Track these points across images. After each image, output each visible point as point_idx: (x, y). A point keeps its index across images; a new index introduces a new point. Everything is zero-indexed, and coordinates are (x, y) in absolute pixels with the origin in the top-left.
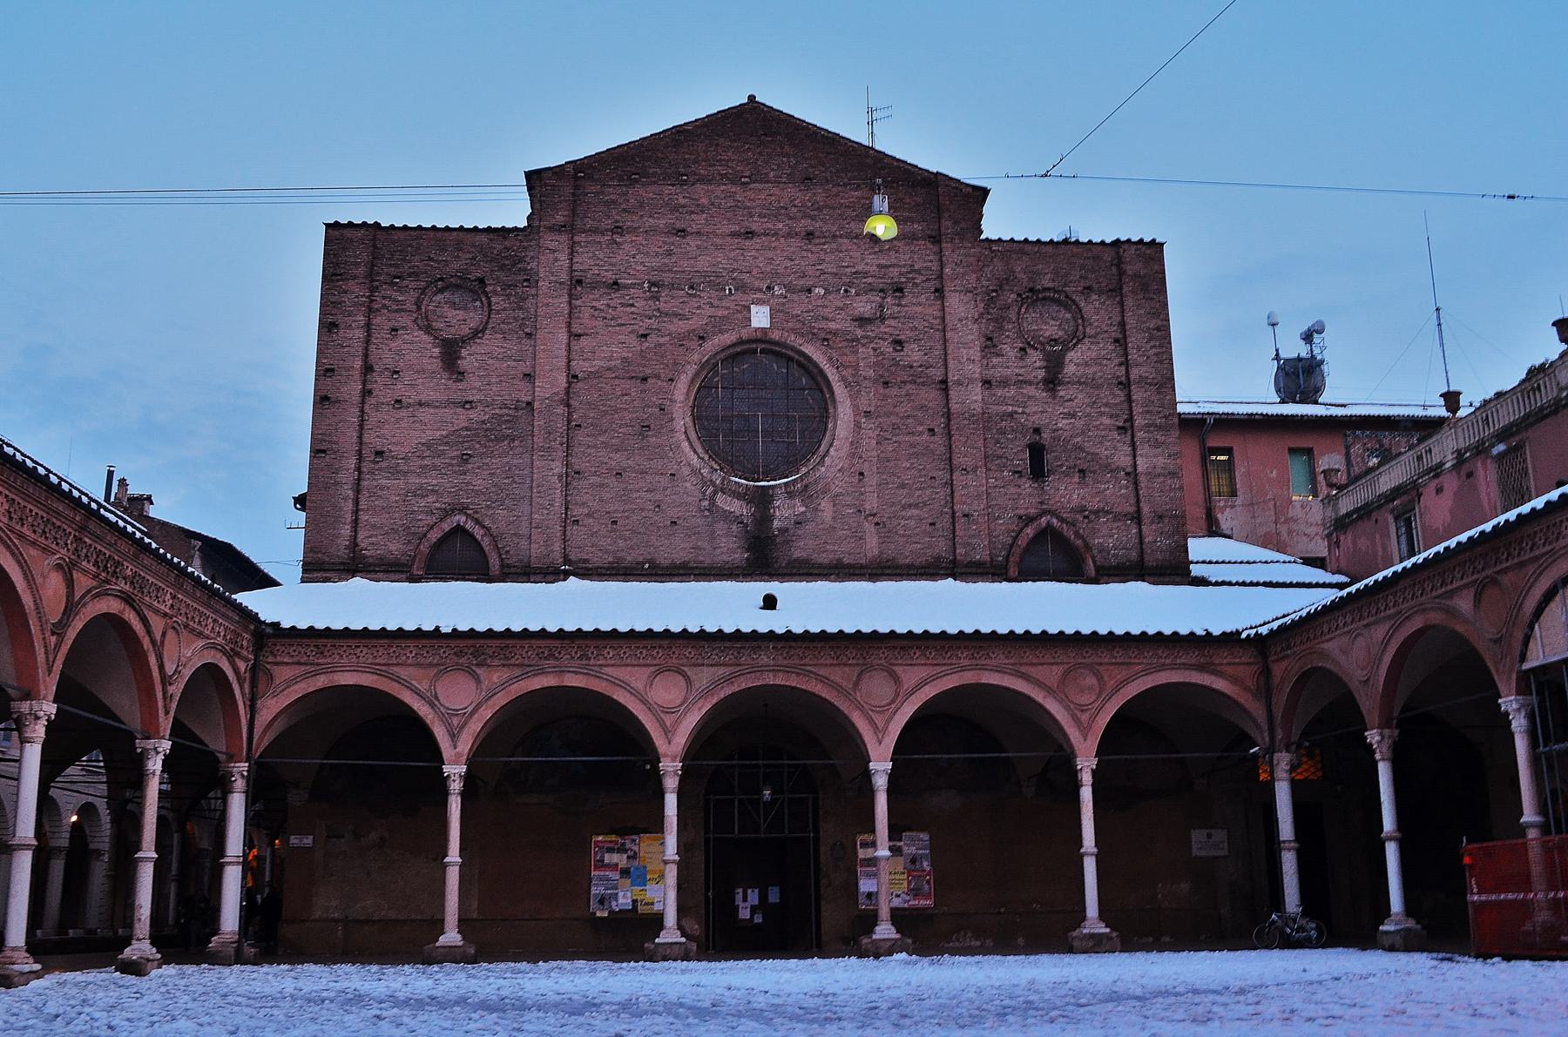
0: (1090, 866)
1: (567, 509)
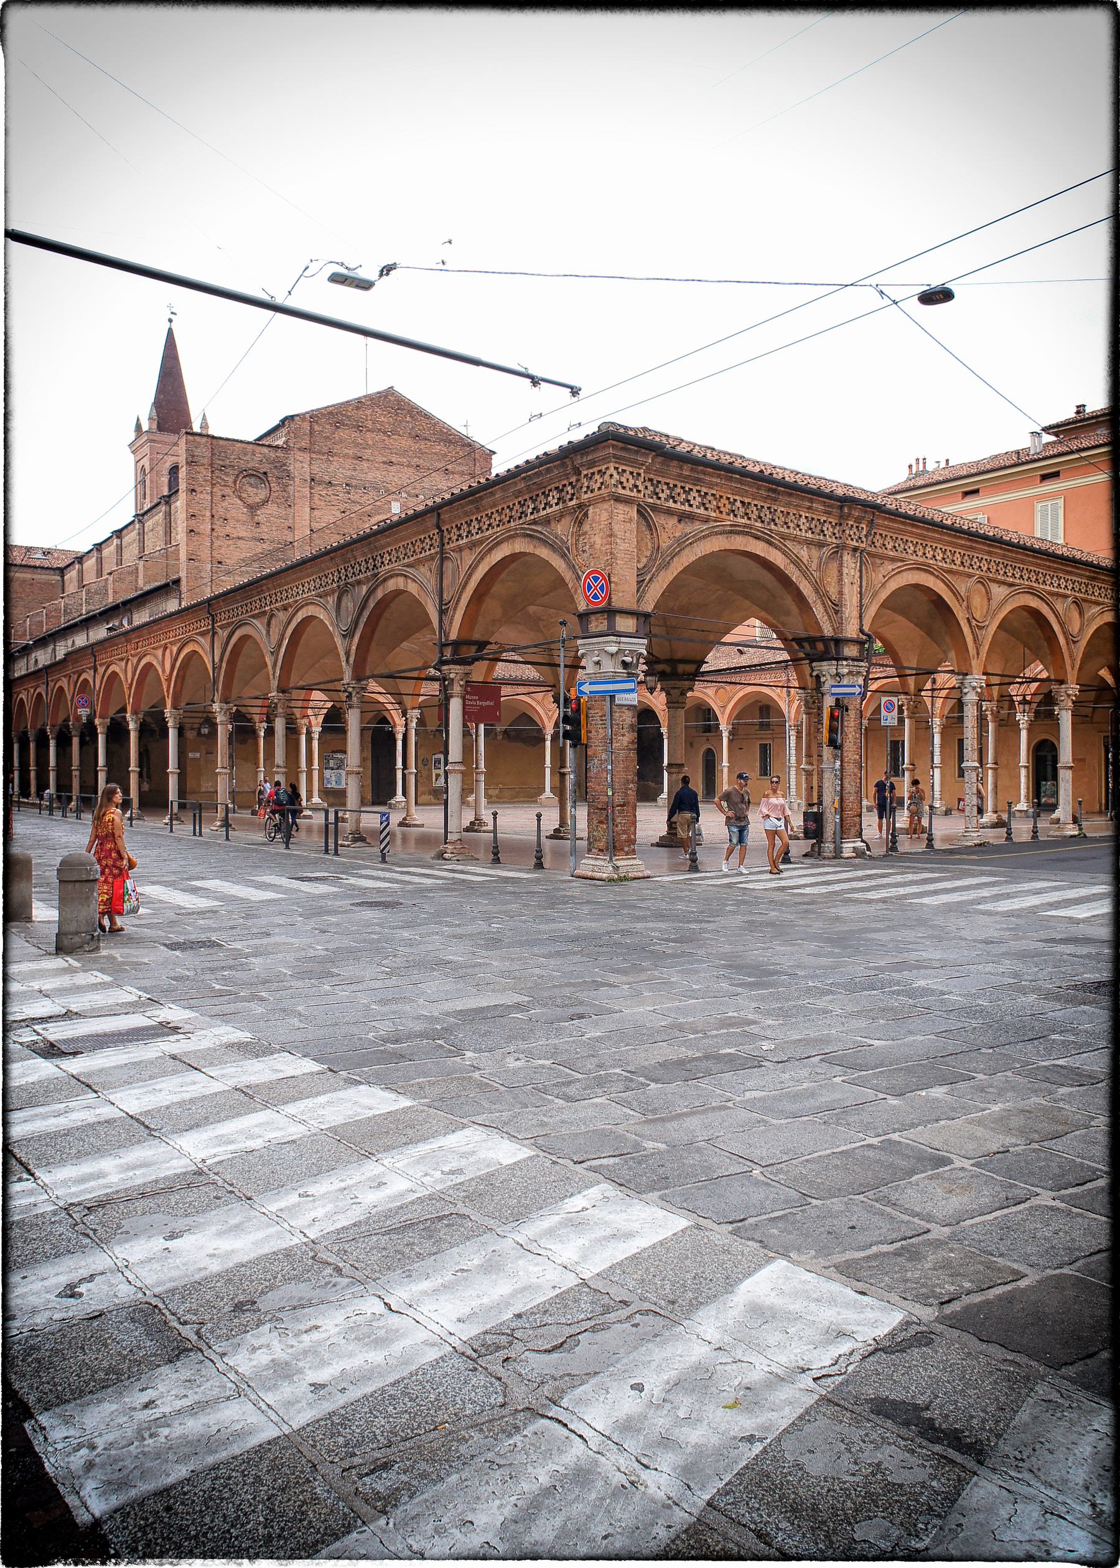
0: (548, 772)
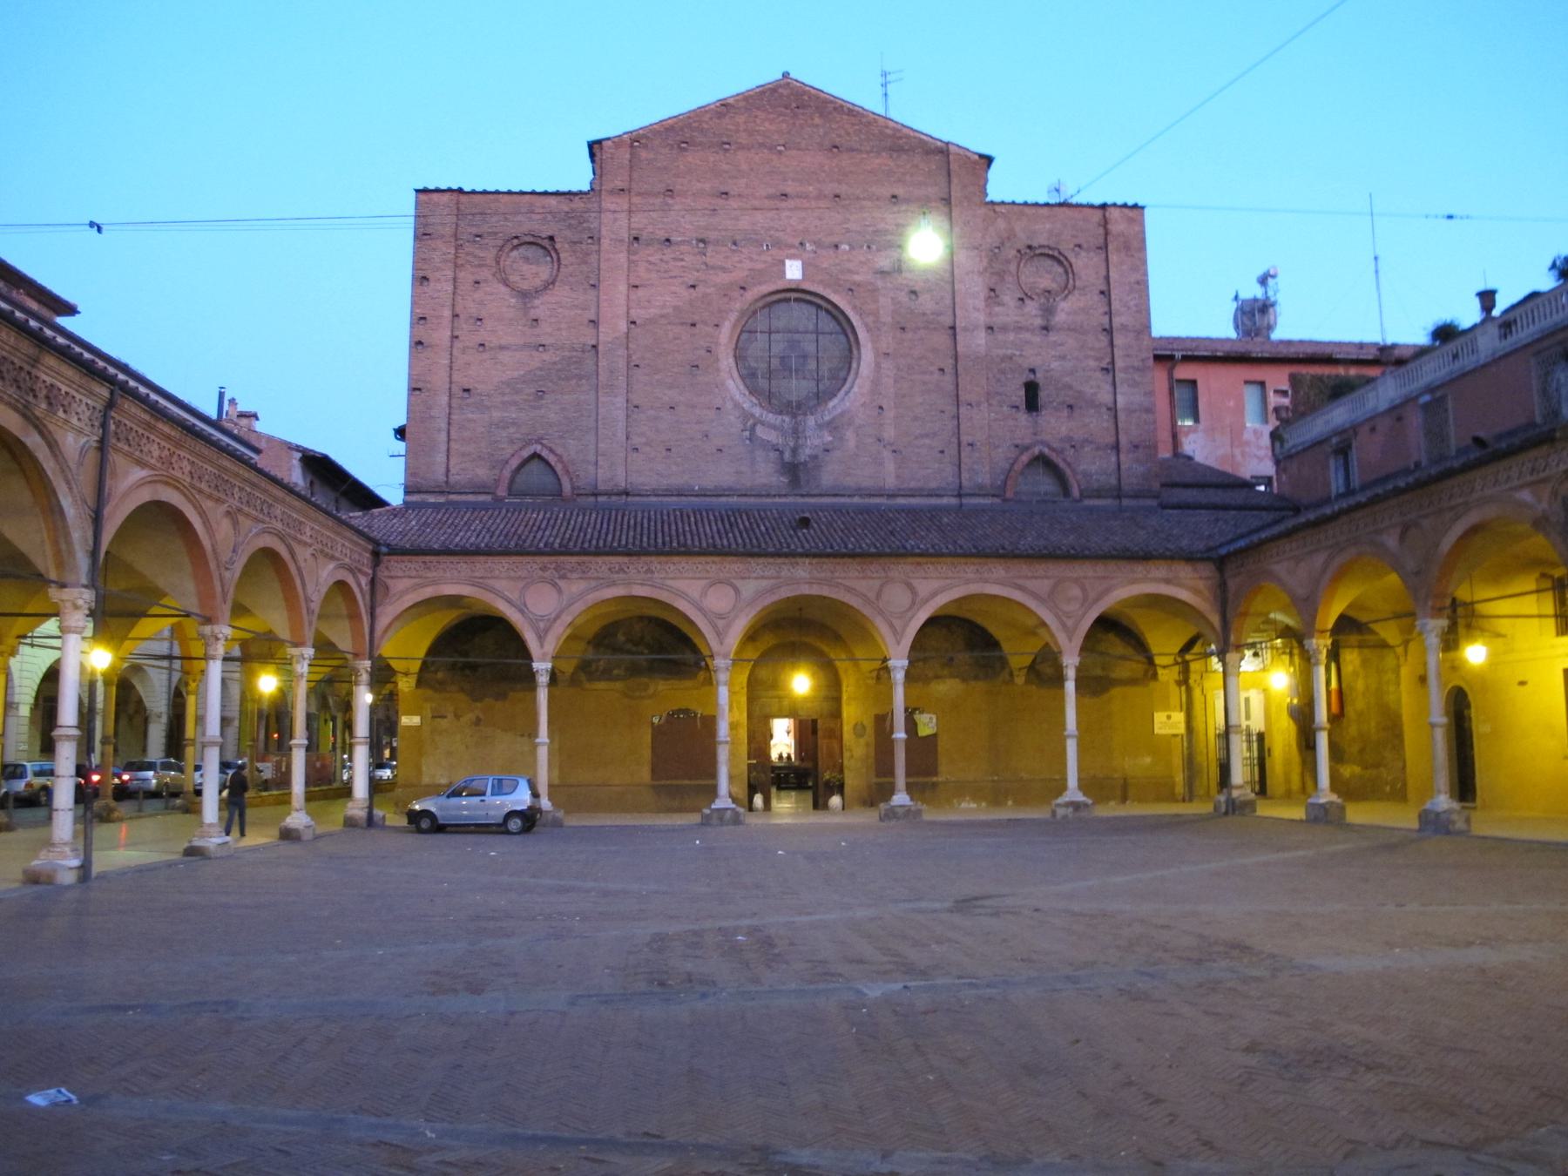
1: (627, 438)
